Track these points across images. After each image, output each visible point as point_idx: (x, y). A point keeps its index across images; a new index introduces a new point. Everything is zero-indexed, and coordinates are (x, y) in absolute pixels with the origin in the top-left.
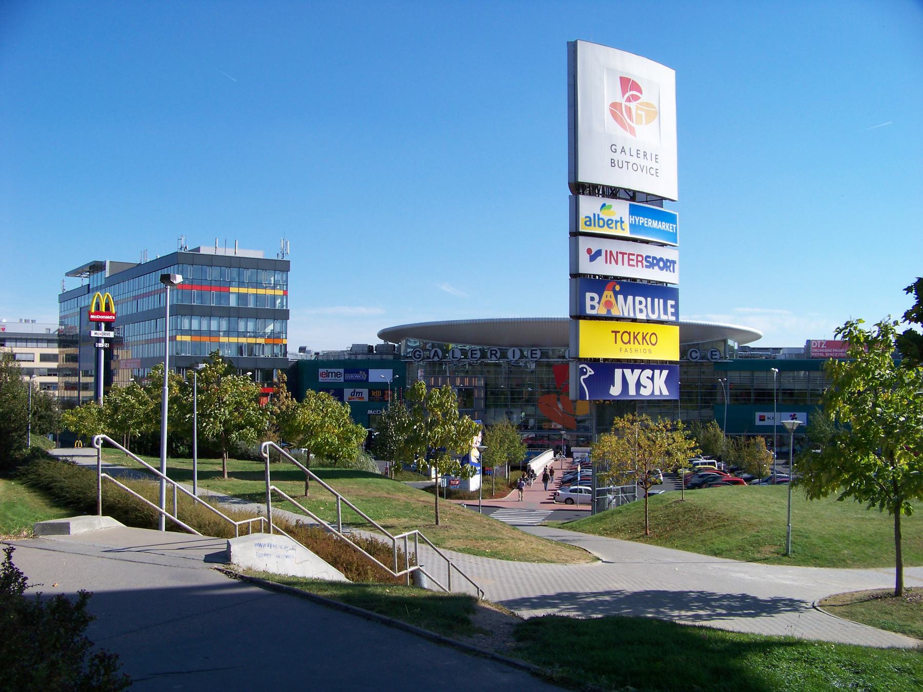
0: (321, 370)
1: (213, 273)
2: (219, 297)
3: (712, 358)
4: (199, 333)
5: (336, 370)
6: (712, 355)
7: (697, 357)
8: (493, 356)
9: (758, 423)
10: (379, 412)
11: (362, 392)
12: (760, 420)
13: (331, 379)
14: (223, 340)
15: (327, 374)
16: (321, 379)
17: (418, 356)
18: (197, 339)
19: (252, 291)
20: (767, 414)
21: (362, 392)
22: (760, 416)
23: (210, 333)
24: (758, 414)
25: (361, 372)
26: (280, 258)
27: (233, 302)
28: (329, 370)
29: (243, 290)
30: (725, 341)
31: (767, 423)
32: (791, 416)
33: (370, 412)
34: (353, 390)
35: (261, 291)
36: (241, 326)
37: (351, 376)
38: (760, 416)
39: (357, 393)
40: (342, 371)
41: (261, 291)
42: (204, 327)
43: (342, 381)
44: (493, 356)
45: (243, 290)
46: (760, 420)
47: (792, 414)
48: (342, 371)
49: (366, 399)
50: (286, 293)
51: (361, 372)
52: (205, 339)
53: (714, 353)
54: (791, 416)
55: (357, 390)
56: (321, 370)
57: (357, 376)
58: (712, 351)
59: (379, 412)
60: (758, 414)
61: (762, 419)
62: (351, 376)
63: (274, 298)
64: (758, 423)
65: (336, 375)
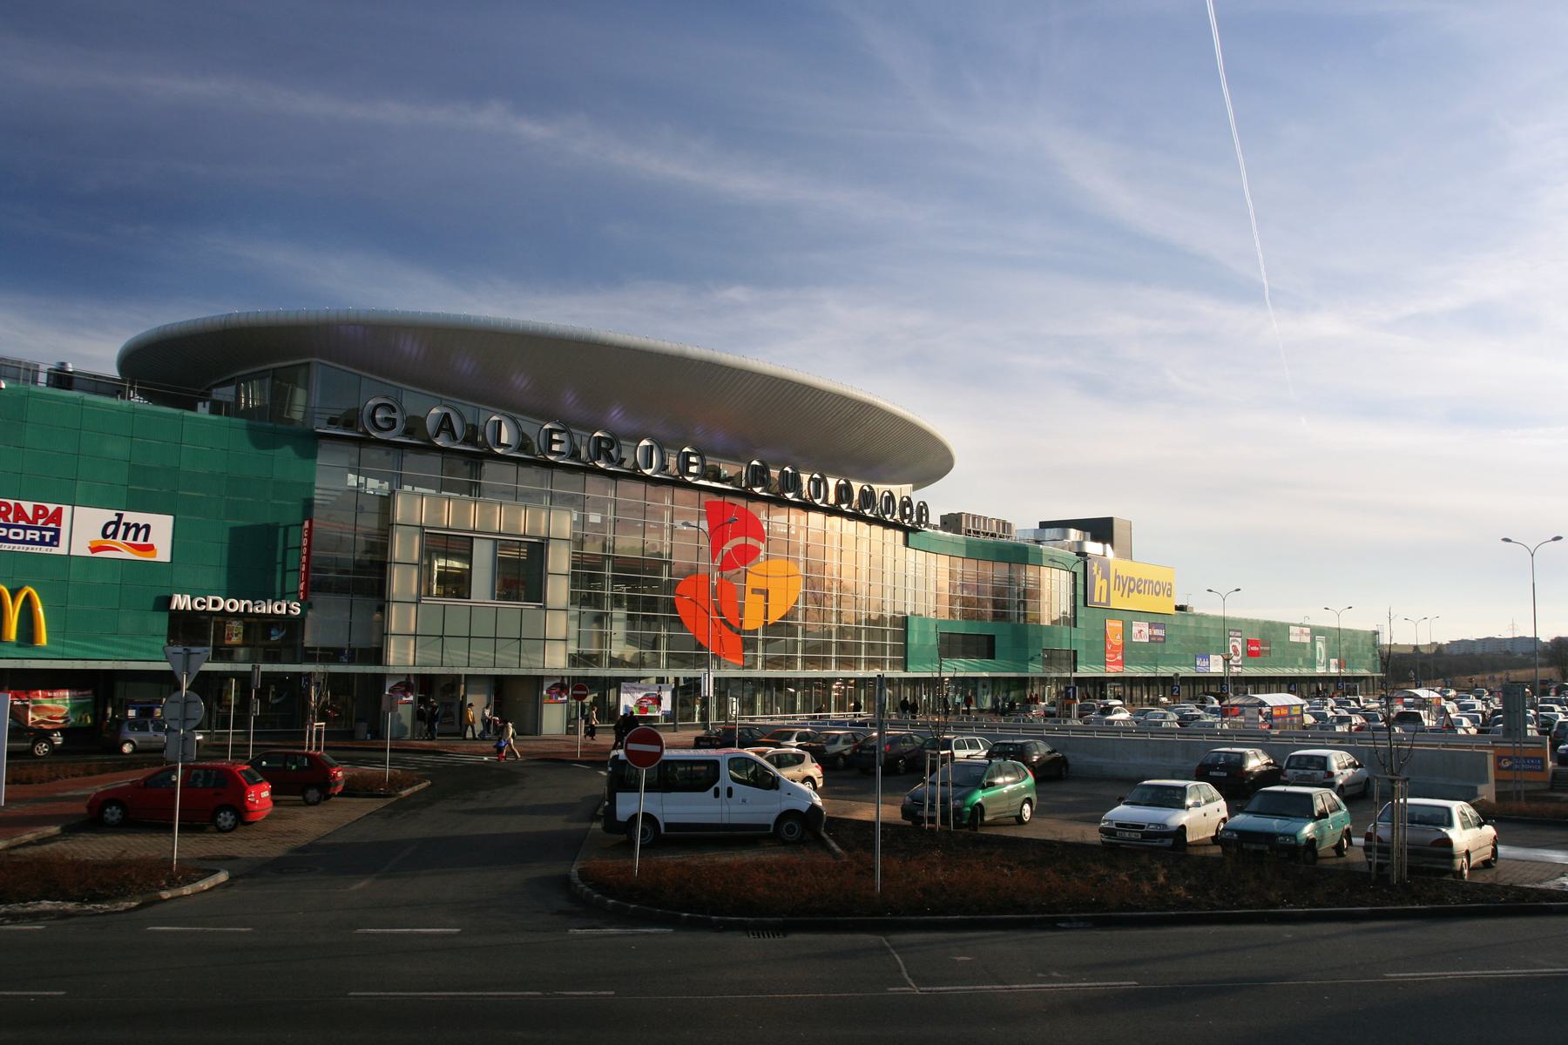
10: (215, 603)
34: (110, 515)
39: (127, 525)
49: (163, 554)
55: (130, 517)
59: (215, 603)
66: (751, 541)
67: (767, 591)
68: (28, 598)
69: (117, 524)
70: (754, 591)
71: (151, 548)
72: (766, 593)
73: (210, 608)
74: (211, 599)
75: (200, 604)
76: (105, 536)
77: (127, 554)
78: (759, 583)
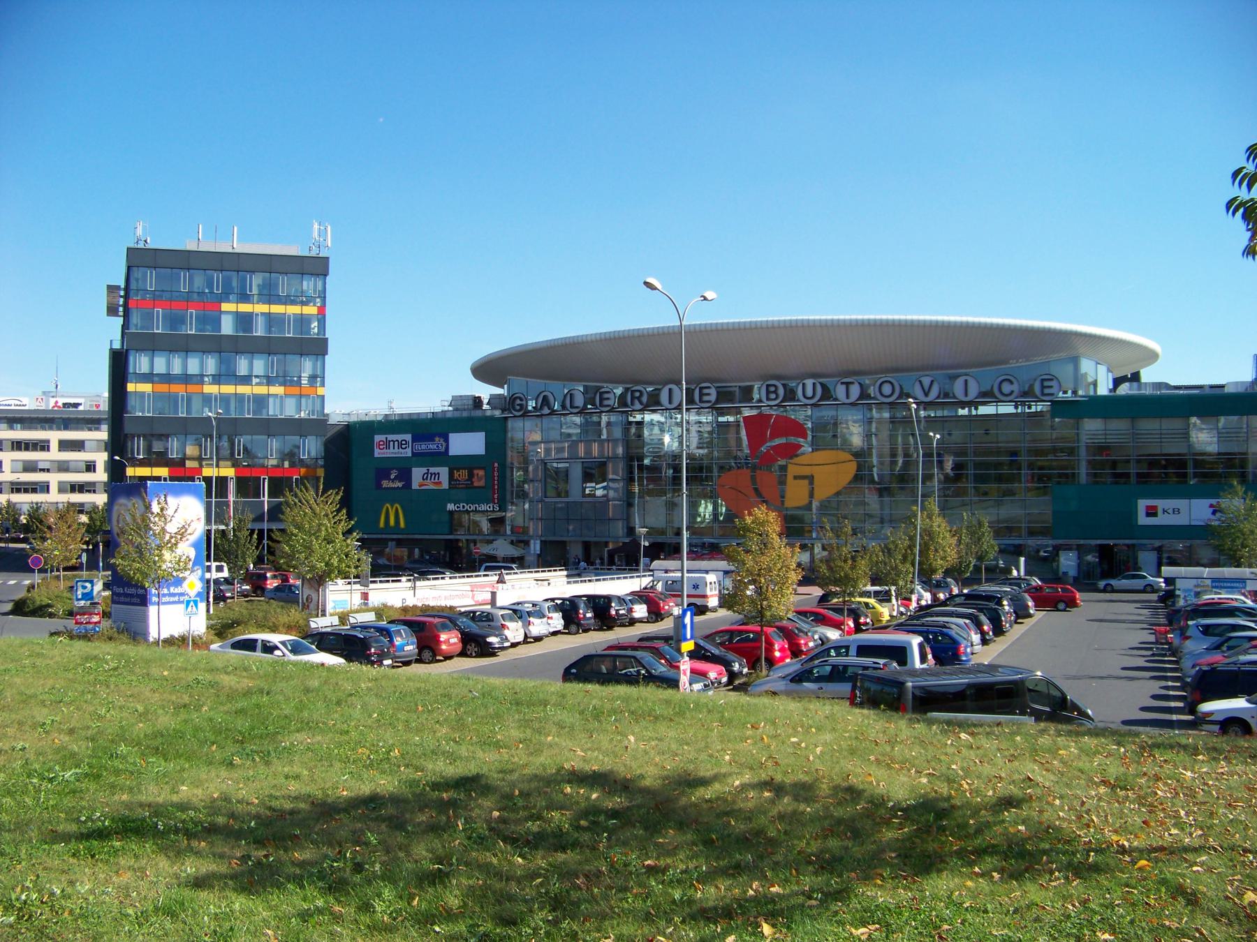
0: (378, 438)
1: (184, 283)
2: (202, 321)
3: (1043, 394)
4: (167, 378)
5: (400, 437)
6: (1043, 387)
7: (1012, 392)
8: (636, 402)
9: (1143, 520)
10: (464, 507)
11: (438, 474)
12: (1148, 515)
13: (393, 452)
14: (210, 389)
15: (387, 444)
16: (378, 453)
17: (518, 408)
18: (163, 388)
19: (264, 308)
20: (1161, 504)
21: (438, 474)
22: (1148, 508)
23: (186, 379)
24: (1142, 504)
25: (437, 439)
26: (313, 254)
27: (227, 327)
28: (391, 437)
29: (245, 308)
30: (1075, 361)
31: (1161, 520)
32: (1211, 506)
33: (451, 507)
34: (424, 470)
35: (277, 309)
36: (242, 366)
37: (423, 447)
38: (1148, 508)
40: (408, 437)
41: (277, 309)
42: (177, 369)
43: (410, 454)
44: (636, 402)
45: (245, 308)
46: (1148, 515)
47: (1214, 502)
48: (408, 437)
49: (445, 485)
50: (322, 310)
51: (437, 439)
52: (179, 389)
53: (1046, 384)
54: (1211, 506)
55: (432, 470)
56: (378, 438)
57: (432, 446)
58: (1043, 380)
59: (464, 507)
60: (1142, 504)
61: (1151, 512)
62: (423, 447)
63: (303, 321)
64: (1143, 520)
65: (400, 445)
66: (792, 439)
67: (813, 477)
68: (397, 508)
69: (427, 473)
70: (796, 478)
71: (440, 483)
72: (811, 479)
73: (461, 509)
74: (461, 505)
75: (458, 507)
76: (423, 479)
77: (432, 487)
78: (806, 471)
